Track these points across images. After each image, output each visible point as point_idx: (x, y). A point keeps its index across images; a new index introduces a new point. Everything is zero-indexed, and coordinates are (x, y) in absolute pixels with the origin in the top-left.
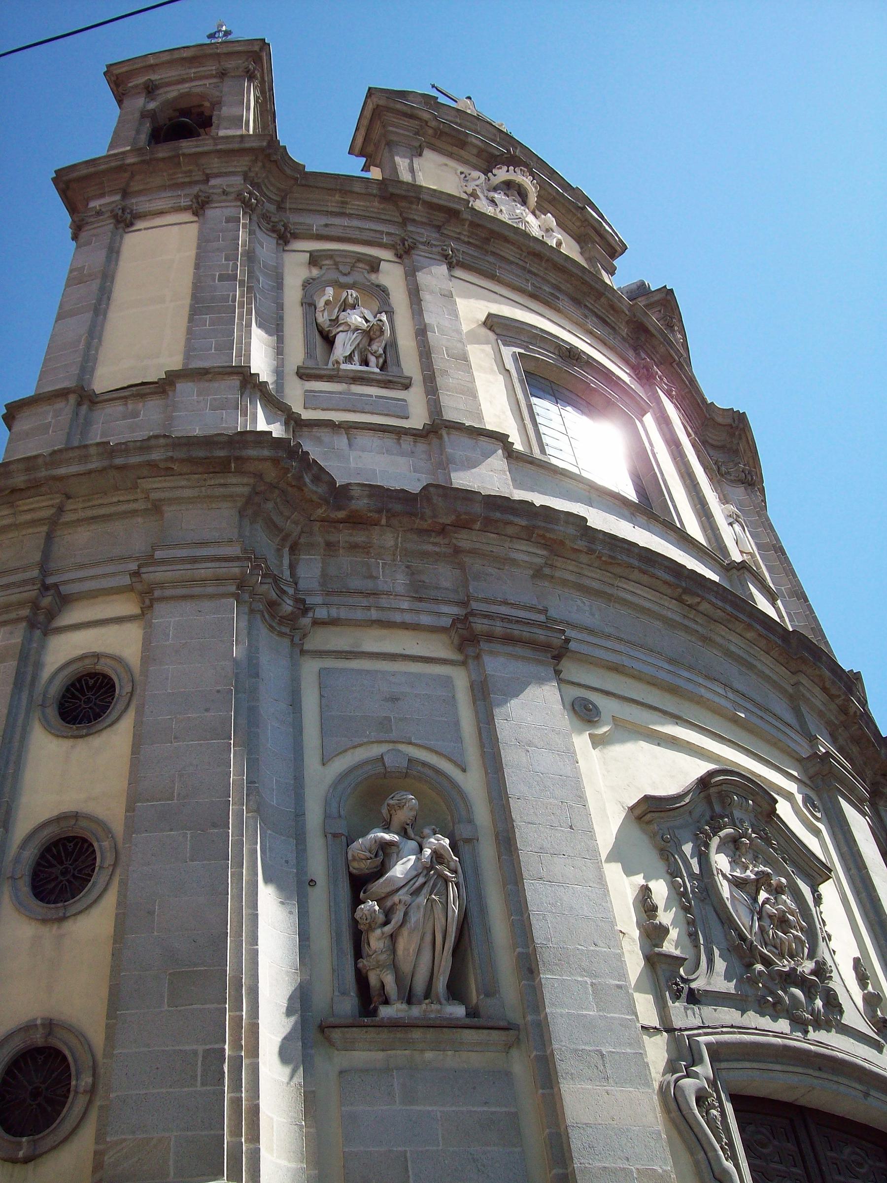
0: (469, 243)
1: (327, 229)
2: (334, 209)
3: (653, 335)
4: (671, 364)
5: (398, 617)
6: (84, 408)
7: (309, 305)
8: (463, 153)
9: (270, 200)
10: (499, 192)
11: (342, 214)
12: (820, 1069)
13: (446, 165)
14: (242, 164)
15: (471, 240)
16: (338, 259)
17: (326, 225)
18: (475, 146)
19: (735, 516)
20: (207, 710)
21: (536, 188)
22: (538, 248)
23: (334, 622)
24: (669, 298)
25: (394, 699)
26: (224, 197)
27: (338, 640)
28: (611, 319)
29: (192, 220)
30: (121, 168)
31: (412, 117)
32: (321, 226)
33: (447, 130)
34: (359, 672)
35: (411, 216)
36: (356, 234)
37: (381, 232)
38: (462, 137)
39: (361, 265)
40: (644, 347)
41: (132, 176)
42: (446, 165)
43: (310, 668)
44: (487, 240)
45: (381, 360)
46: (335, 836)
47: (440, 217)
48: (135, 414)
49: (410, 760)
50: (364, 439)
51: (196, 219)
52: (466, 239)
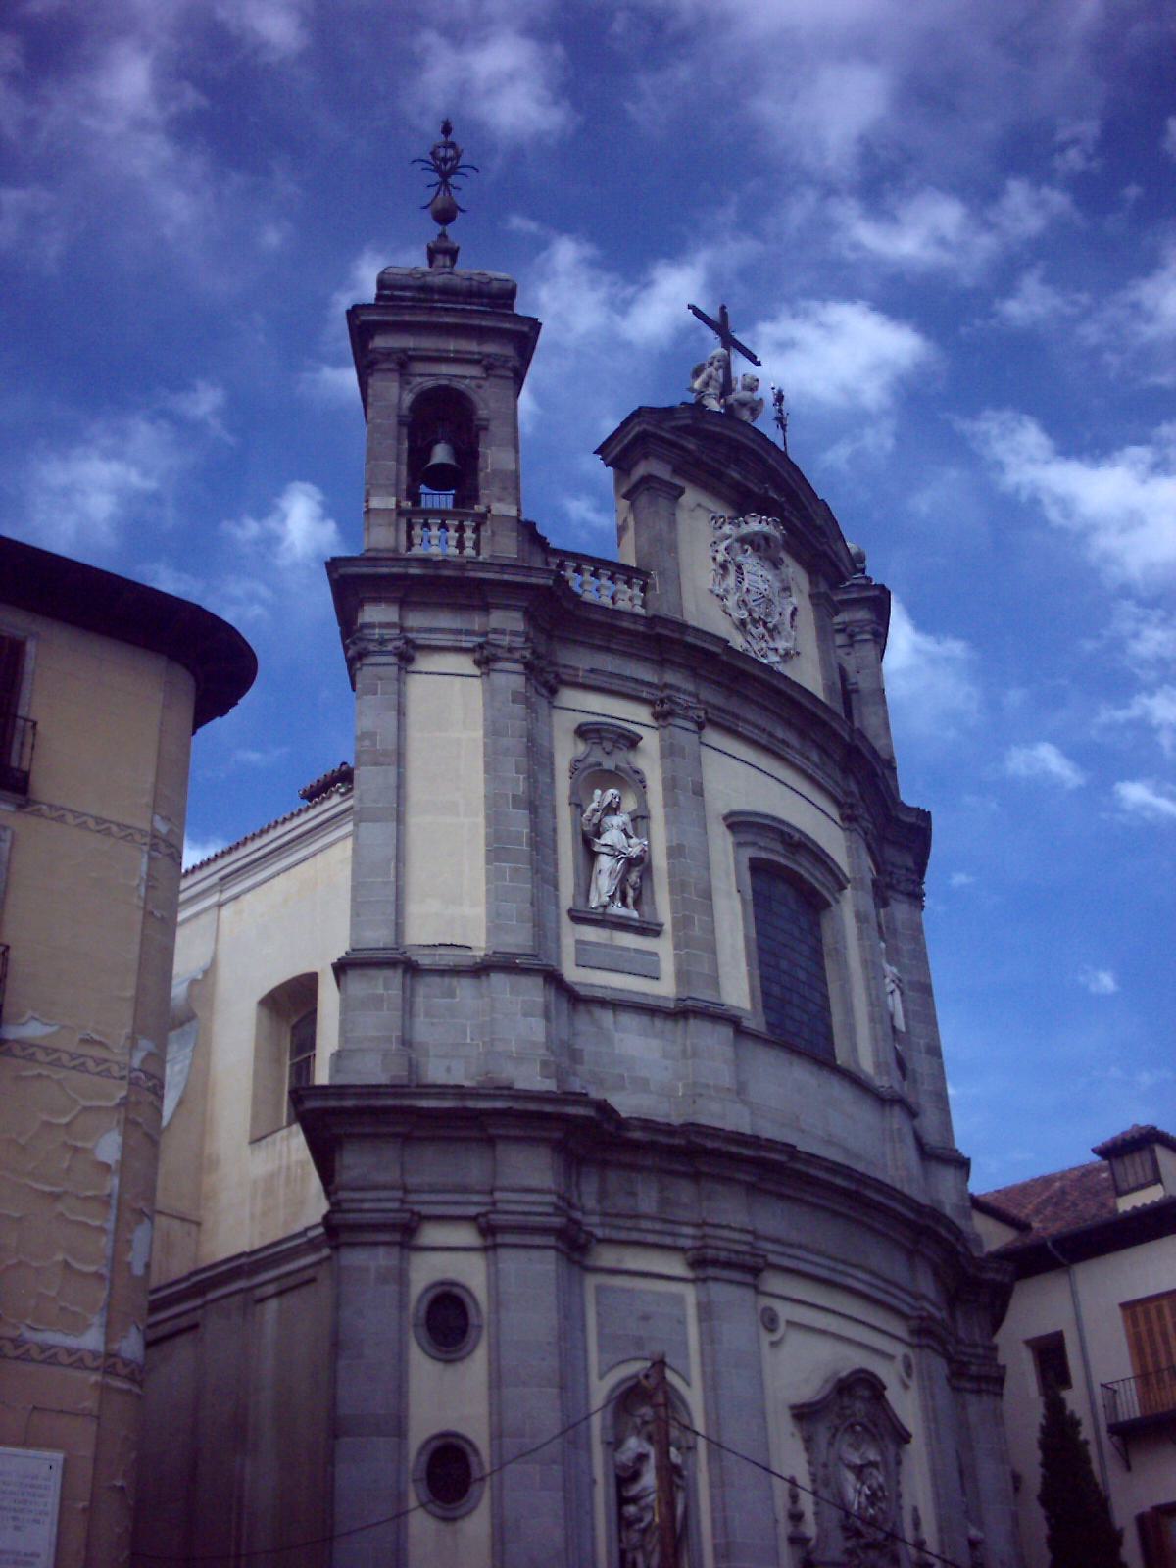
1: (593, 676)
5: (651, 1238)
6: (408, 976)
7: (578, 806)
10: (746, 547)
13: (699, 505)
16: (603, 734)
17: (592, 671)
19: (897, 981)
20: (543, 1359)
25: (645, 1318)
26: (507, 655)
27: (607, 1257)
29: (473, 673)
32: (587, 671)
34: (624, 1290)
36: (616, 685)
39: (622, 741)
42: (699, 505)
43: (592, 1281)
45: (637, 892)
46: (609, 1443)
48: (451, 994)
50: (628, 1020)
51: (477, 672)
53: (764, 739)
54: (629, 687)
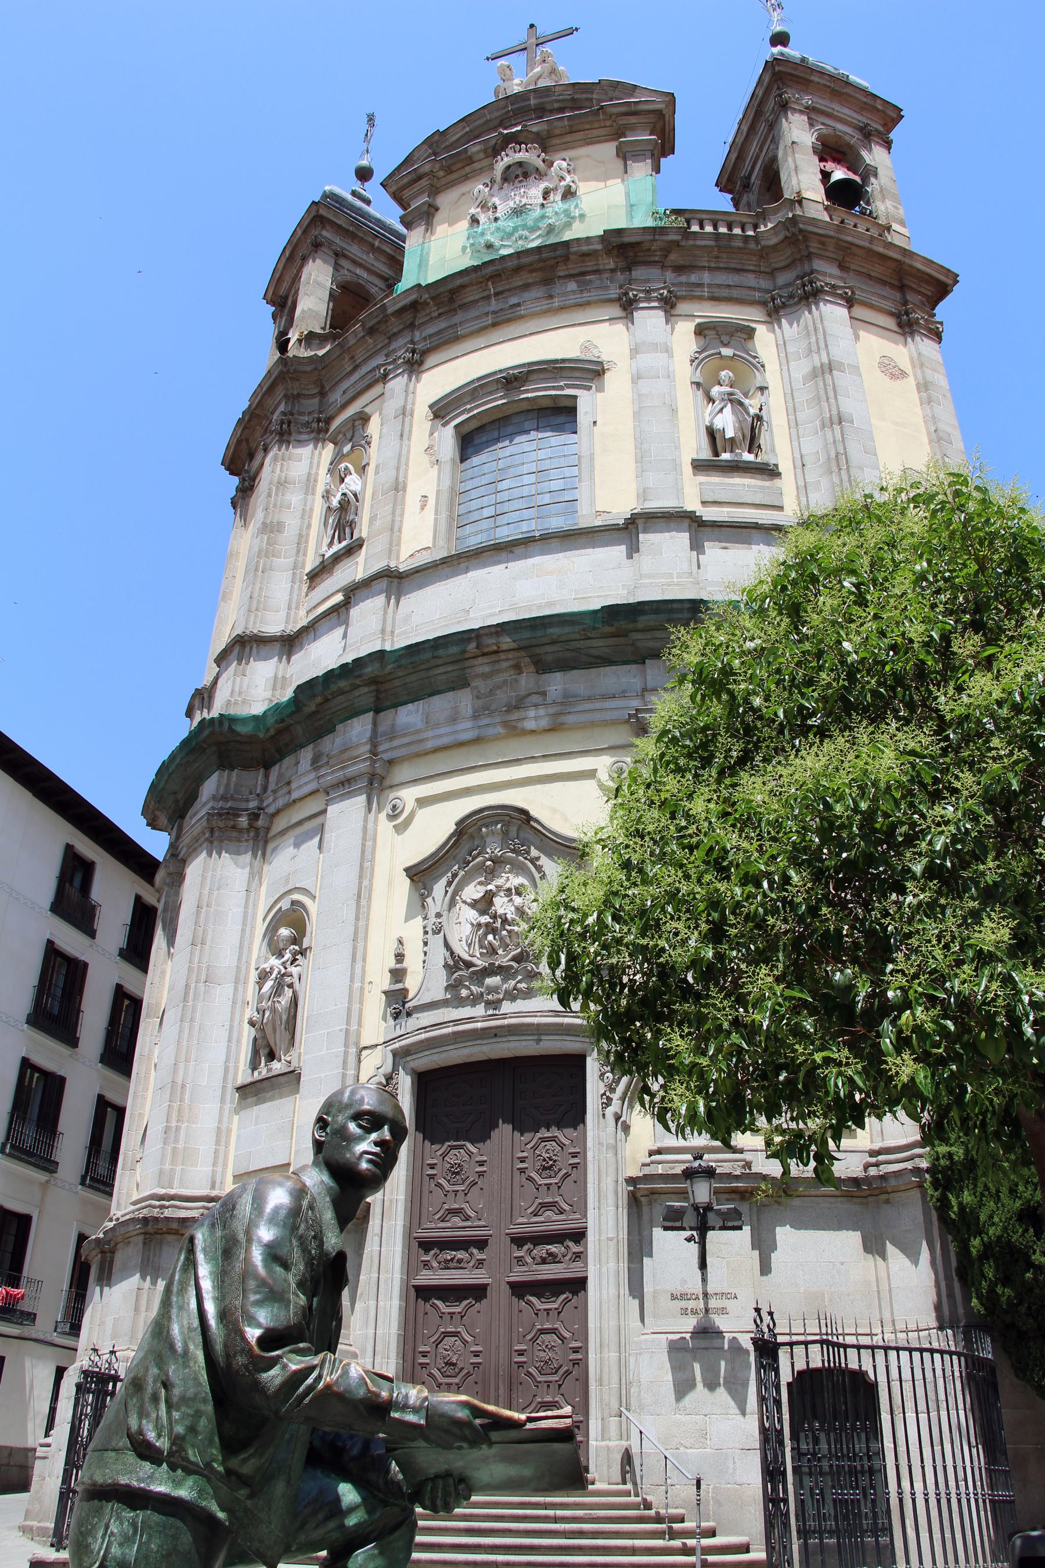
0: (440, 315)
2: (349, 369)
3: (638, 244)
4: (678, 246)
8: (476, 166)
9: (313, 396)
11: (356, 368)
12: (496, 1035)
13: (463, 194)
14: (280, 392)
15: (441, 311)
16: (343, 430)
18: (478, 152)
21: (535, 148)
22: (489, 270)
23: (278, 812)
24: (777, 68)
28: (590, 265)
30: (239, 442)
31: (420, 178)
33: (450, 162)
35: (392, 332)
37: (374, 370)
38: (463, 156)
39: (357, 423)
40: (640, 259)
41: (247, 440)
42: (463, 194)
44: (451, 300)
47: (408, 317)
49: (293, 903)
52: (436, 314)
53: (490, 320)
54: (366, 382)
